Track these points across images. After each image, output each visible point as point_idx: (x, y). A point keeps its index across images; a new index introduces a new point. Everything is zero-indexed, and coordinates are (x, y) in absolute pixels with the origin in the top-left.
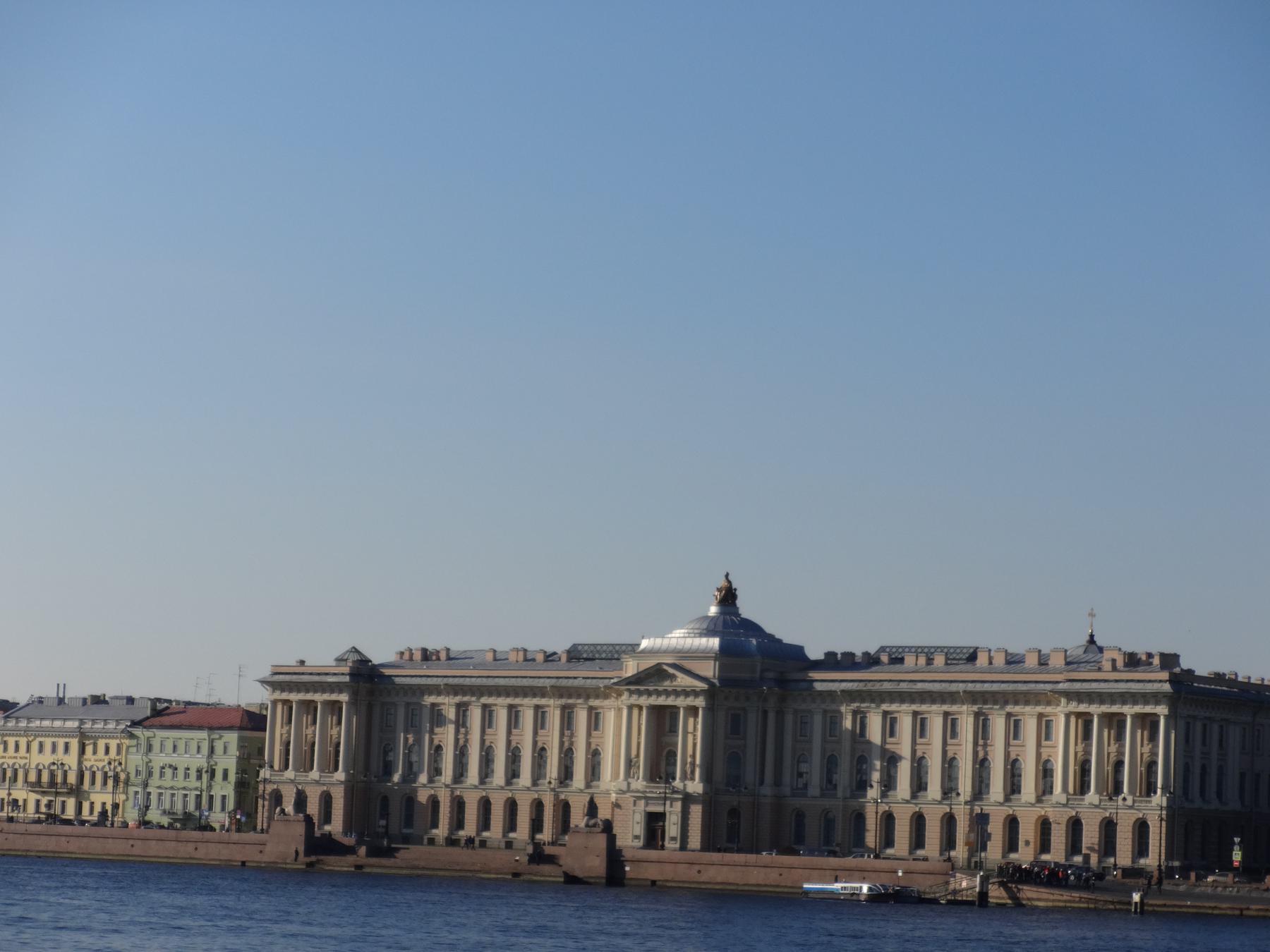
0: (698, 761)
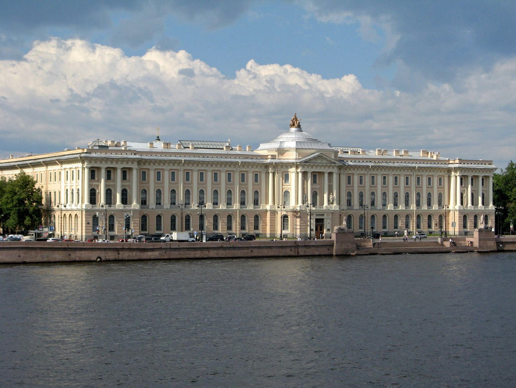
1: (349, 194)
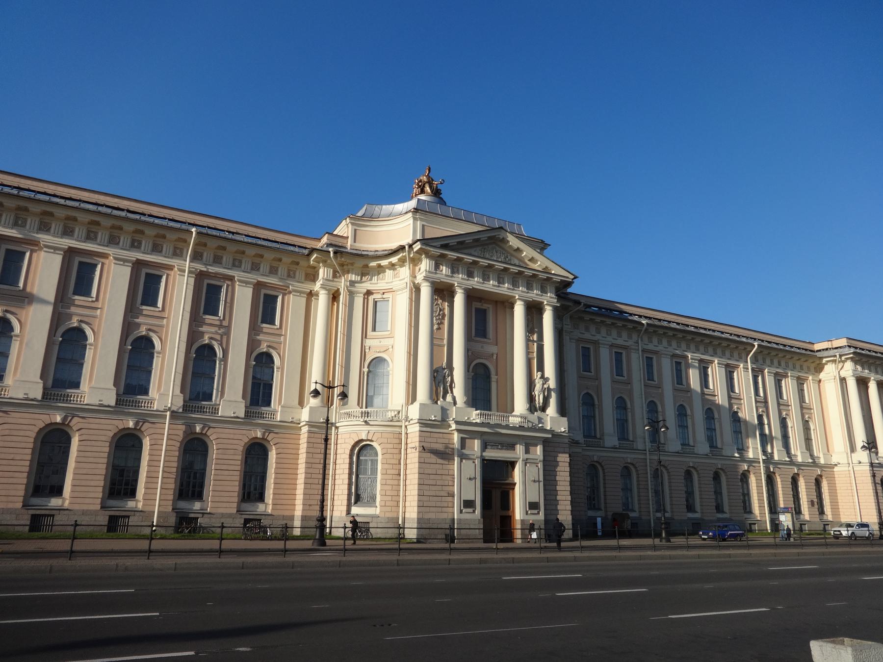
0: (552, 384)
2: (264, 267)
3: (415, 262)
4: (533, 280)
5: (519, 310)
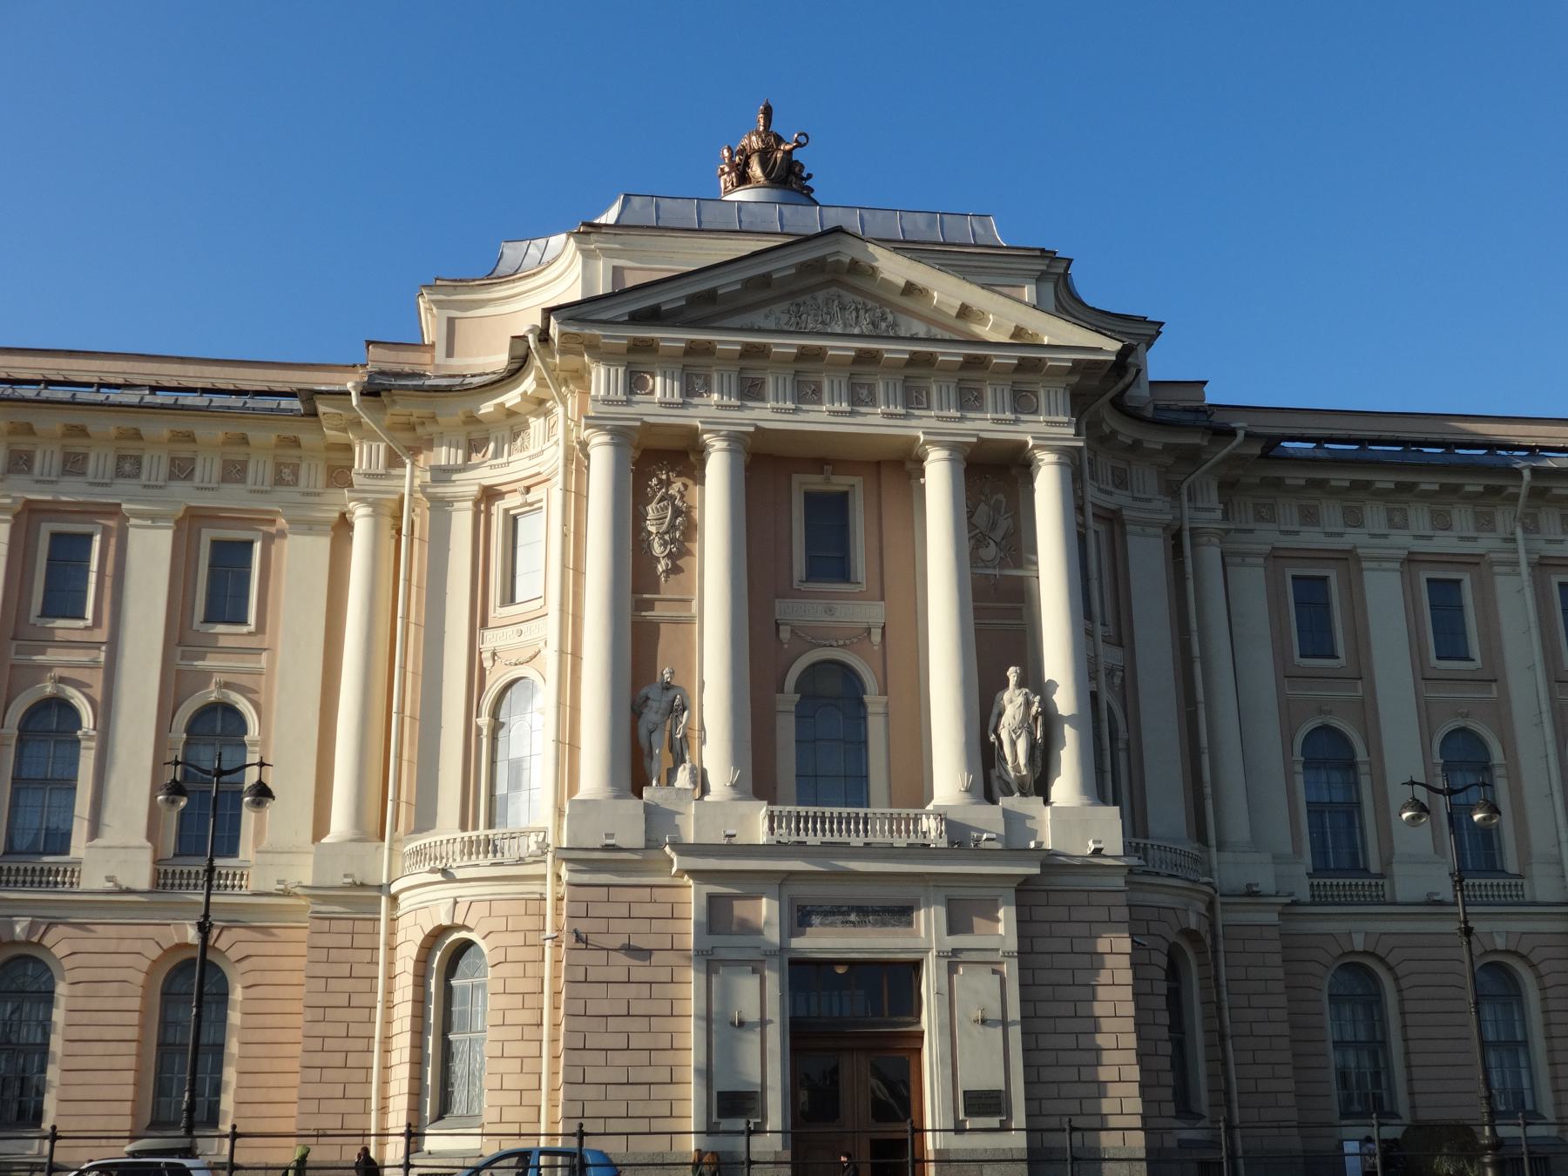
0: (1064, 701)
1: (1330, 755)
2: (208, 467)
3: (579, 377)
4: (972, 374)
5: (937, 477)
